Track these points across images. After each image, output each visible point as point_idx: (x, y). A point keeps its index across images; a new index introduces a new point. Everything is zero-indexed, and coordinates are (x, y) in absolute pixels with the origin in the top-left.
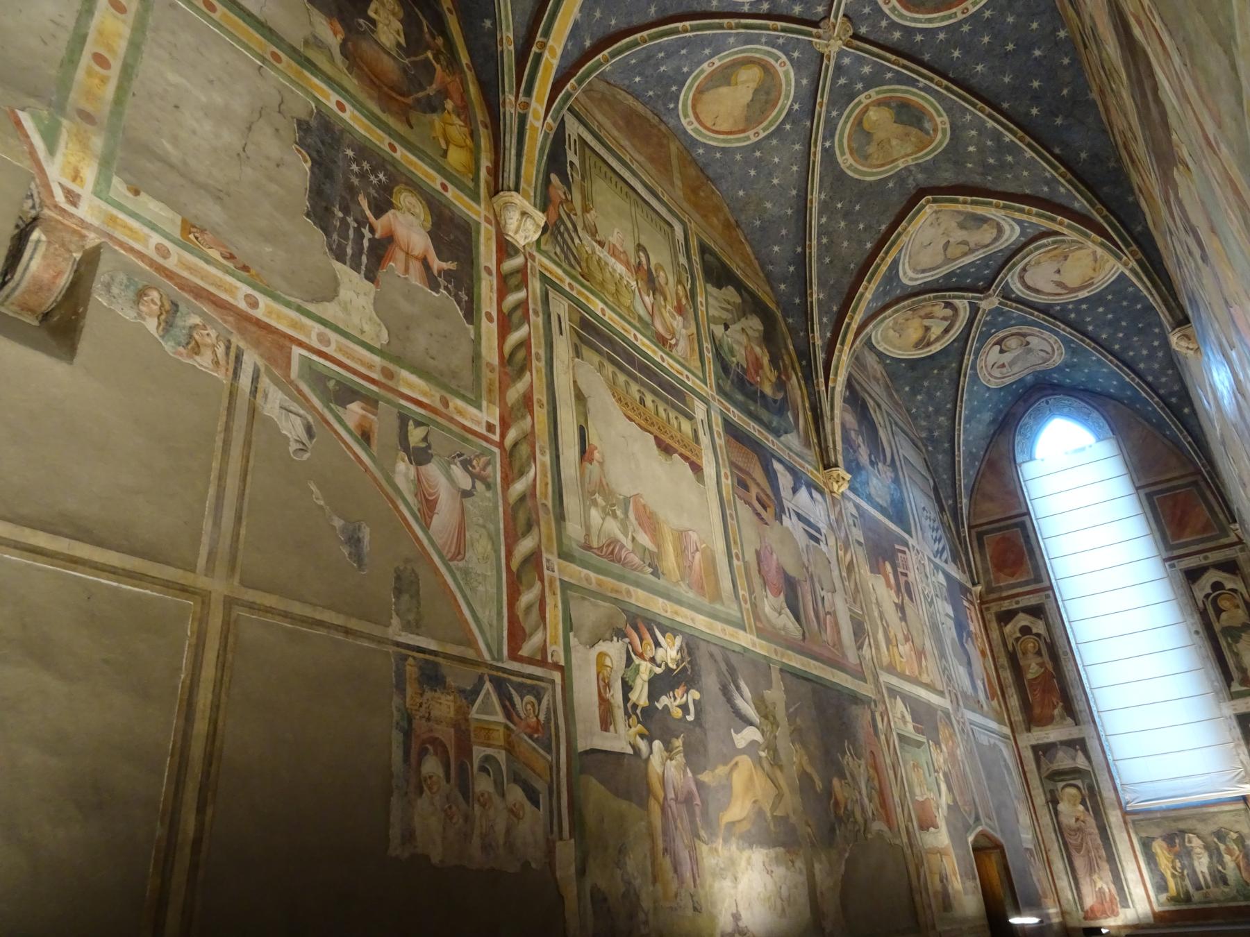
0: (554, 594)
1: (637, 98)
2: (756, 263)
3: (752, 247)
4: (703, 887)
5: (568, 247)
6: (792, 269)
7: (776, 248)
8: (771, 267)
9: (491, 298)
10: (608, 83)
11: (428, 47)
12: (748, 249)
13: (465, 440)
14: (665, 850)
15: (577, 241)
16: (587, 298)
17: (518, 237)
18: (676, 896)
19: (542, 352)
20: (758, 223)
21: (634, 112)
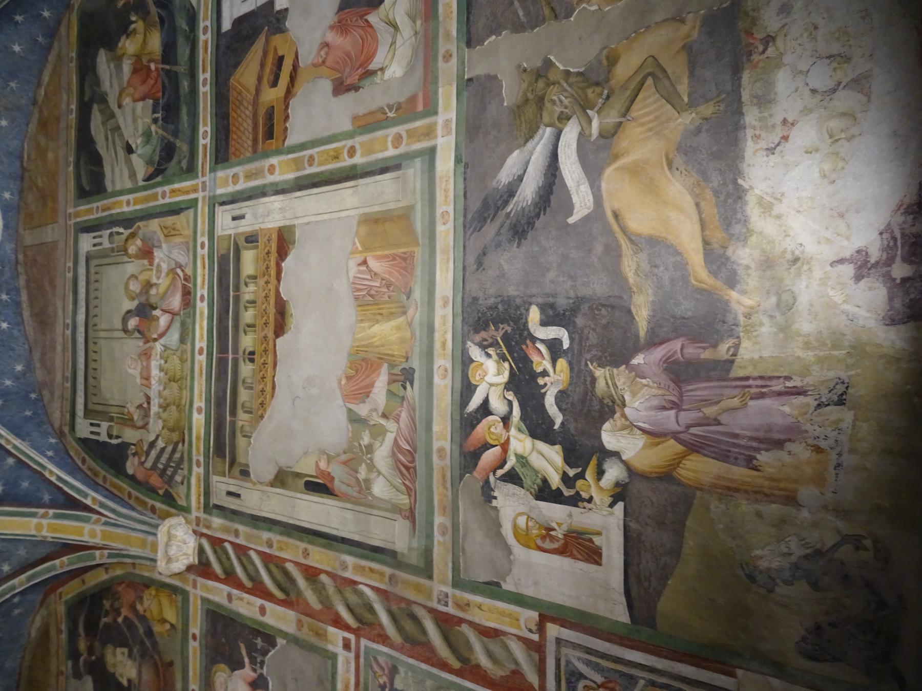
0: (468, 605)
1: (18, 304)
2: (52, 58)
3: (40, 73)
4: (805, 371)
5: (170, 459)
6: (19, 18)
7: (17, 48)
8: (40, 39)
9: (248, 603)
10: (31, 351)
11: (115, 621)
12: (46, 78)
13: (366, 679)
14: (750, 463)
15: (160, 444)
16: (198, 438)
17: (190, 551)
18: (818, 450)
19: (266, 535)
20: (13, 84)
21: (34, 315)
